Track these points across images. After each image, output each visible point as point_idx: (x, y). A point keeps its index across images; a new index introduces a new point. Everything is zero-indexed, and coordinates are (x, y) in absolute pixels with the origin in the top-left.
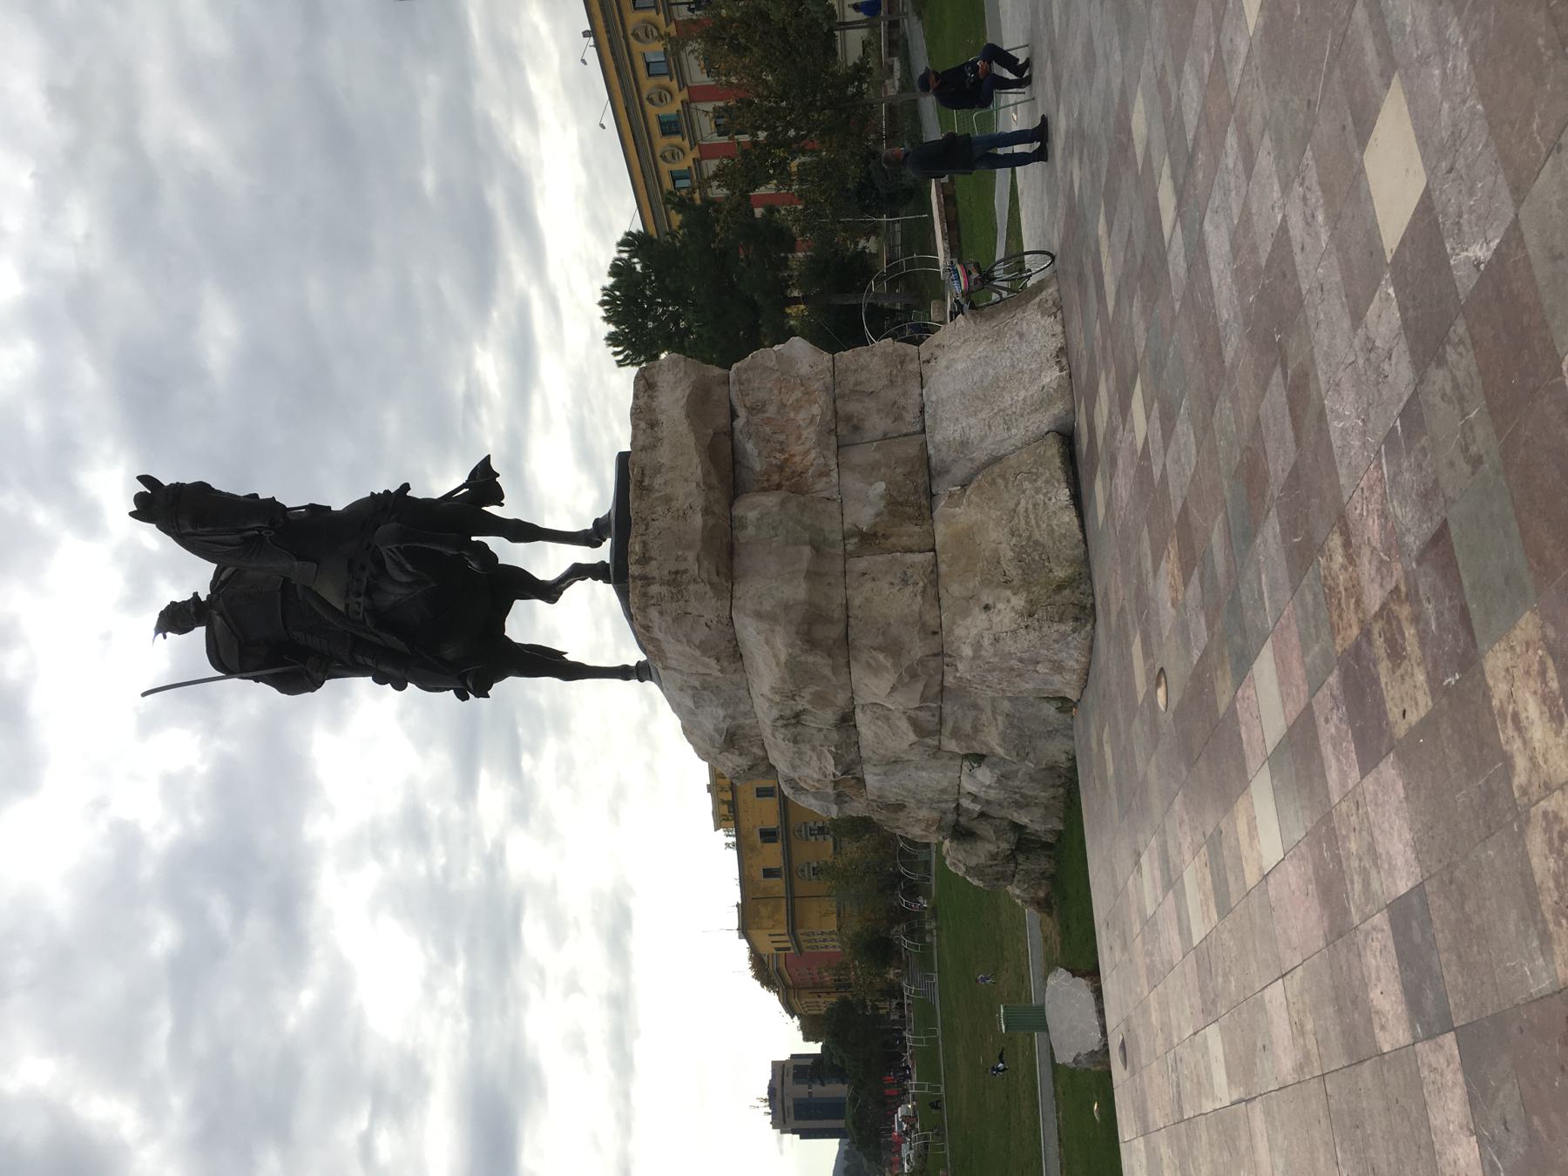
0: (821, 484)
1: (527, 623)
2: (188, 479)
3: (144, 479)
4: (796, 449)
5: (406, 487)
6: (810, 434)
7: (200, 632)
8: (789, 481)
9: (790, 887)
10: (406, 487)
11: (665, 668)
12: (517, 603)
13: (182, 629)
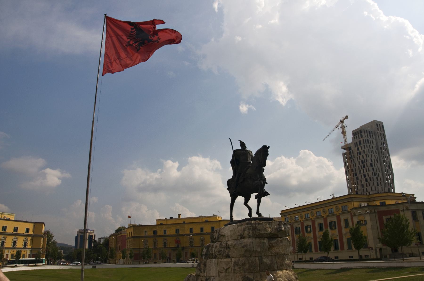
0: (270, 253)
1: (240, 199)
2: (269, 153)
3: (269, 147)
4: (275, 248)
5: (267, 183)
6: (277, 251)
7: (240, 148)
8: (271, 247)
9: (142, 237)
10: (267, 183)
11: (238, 226)
12: (244, 198)
13: (241, 145)
